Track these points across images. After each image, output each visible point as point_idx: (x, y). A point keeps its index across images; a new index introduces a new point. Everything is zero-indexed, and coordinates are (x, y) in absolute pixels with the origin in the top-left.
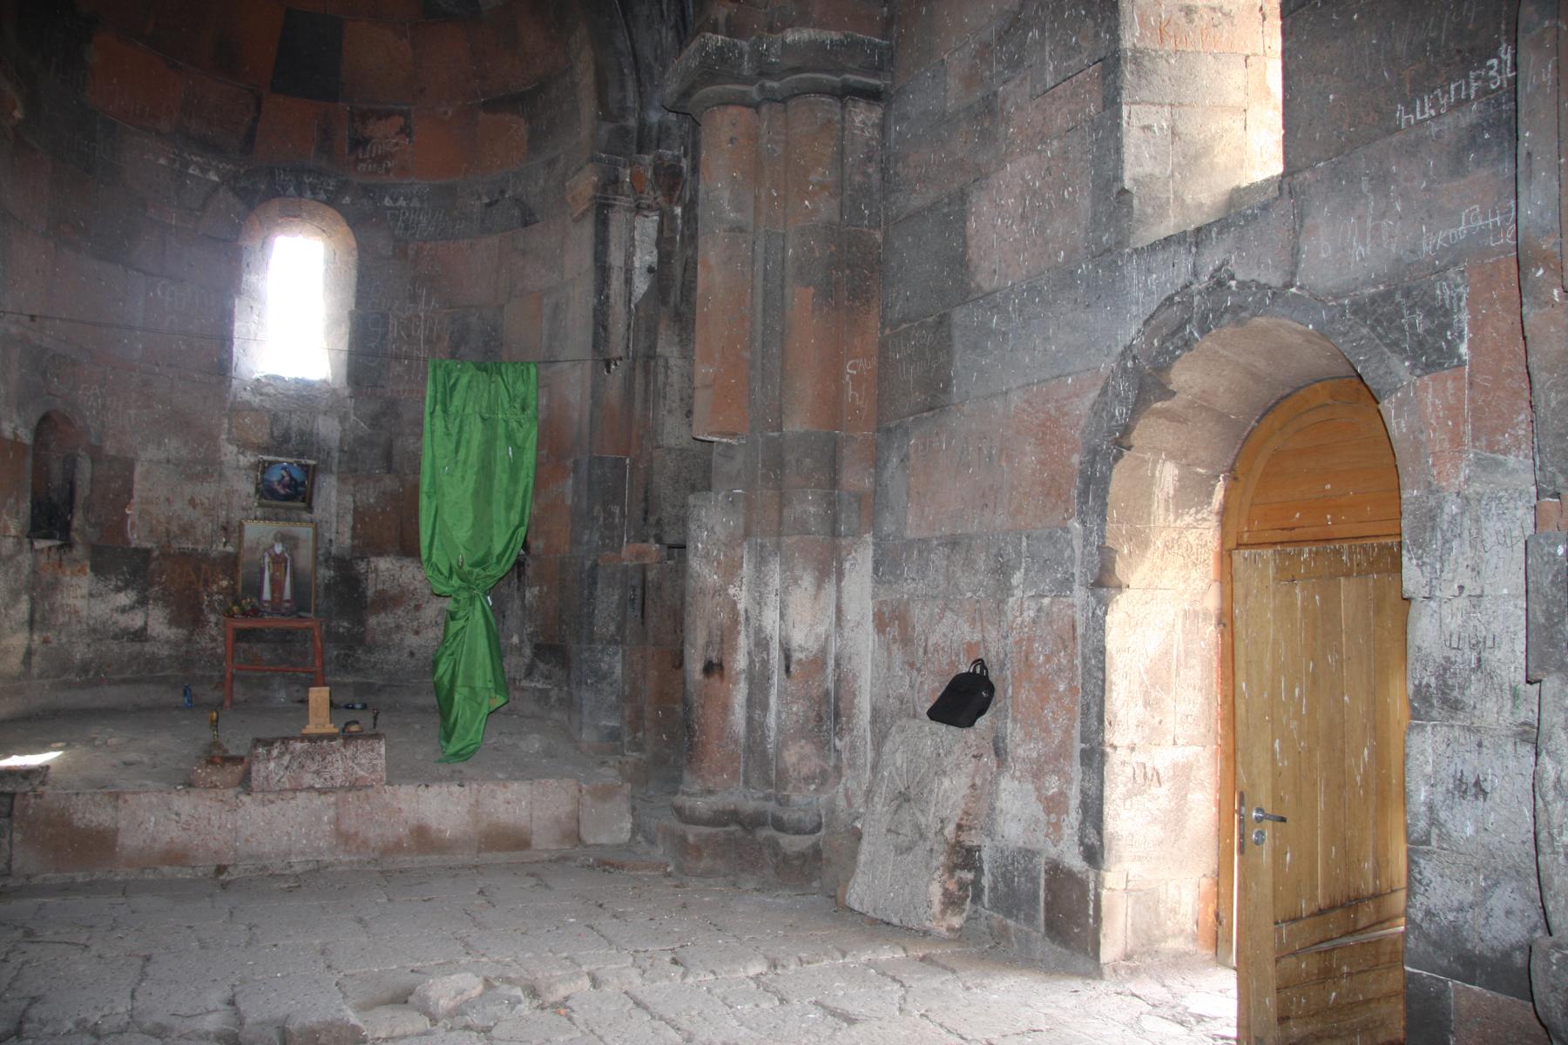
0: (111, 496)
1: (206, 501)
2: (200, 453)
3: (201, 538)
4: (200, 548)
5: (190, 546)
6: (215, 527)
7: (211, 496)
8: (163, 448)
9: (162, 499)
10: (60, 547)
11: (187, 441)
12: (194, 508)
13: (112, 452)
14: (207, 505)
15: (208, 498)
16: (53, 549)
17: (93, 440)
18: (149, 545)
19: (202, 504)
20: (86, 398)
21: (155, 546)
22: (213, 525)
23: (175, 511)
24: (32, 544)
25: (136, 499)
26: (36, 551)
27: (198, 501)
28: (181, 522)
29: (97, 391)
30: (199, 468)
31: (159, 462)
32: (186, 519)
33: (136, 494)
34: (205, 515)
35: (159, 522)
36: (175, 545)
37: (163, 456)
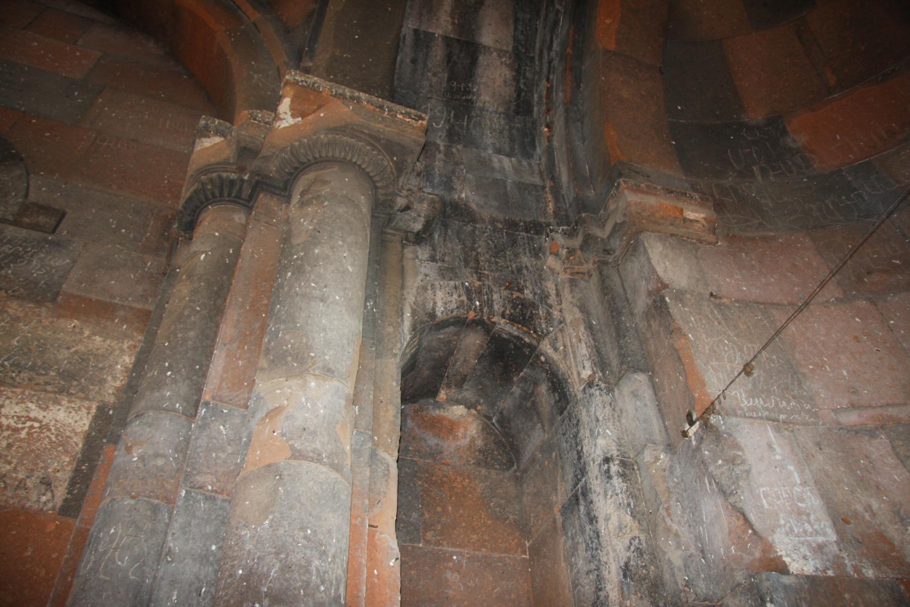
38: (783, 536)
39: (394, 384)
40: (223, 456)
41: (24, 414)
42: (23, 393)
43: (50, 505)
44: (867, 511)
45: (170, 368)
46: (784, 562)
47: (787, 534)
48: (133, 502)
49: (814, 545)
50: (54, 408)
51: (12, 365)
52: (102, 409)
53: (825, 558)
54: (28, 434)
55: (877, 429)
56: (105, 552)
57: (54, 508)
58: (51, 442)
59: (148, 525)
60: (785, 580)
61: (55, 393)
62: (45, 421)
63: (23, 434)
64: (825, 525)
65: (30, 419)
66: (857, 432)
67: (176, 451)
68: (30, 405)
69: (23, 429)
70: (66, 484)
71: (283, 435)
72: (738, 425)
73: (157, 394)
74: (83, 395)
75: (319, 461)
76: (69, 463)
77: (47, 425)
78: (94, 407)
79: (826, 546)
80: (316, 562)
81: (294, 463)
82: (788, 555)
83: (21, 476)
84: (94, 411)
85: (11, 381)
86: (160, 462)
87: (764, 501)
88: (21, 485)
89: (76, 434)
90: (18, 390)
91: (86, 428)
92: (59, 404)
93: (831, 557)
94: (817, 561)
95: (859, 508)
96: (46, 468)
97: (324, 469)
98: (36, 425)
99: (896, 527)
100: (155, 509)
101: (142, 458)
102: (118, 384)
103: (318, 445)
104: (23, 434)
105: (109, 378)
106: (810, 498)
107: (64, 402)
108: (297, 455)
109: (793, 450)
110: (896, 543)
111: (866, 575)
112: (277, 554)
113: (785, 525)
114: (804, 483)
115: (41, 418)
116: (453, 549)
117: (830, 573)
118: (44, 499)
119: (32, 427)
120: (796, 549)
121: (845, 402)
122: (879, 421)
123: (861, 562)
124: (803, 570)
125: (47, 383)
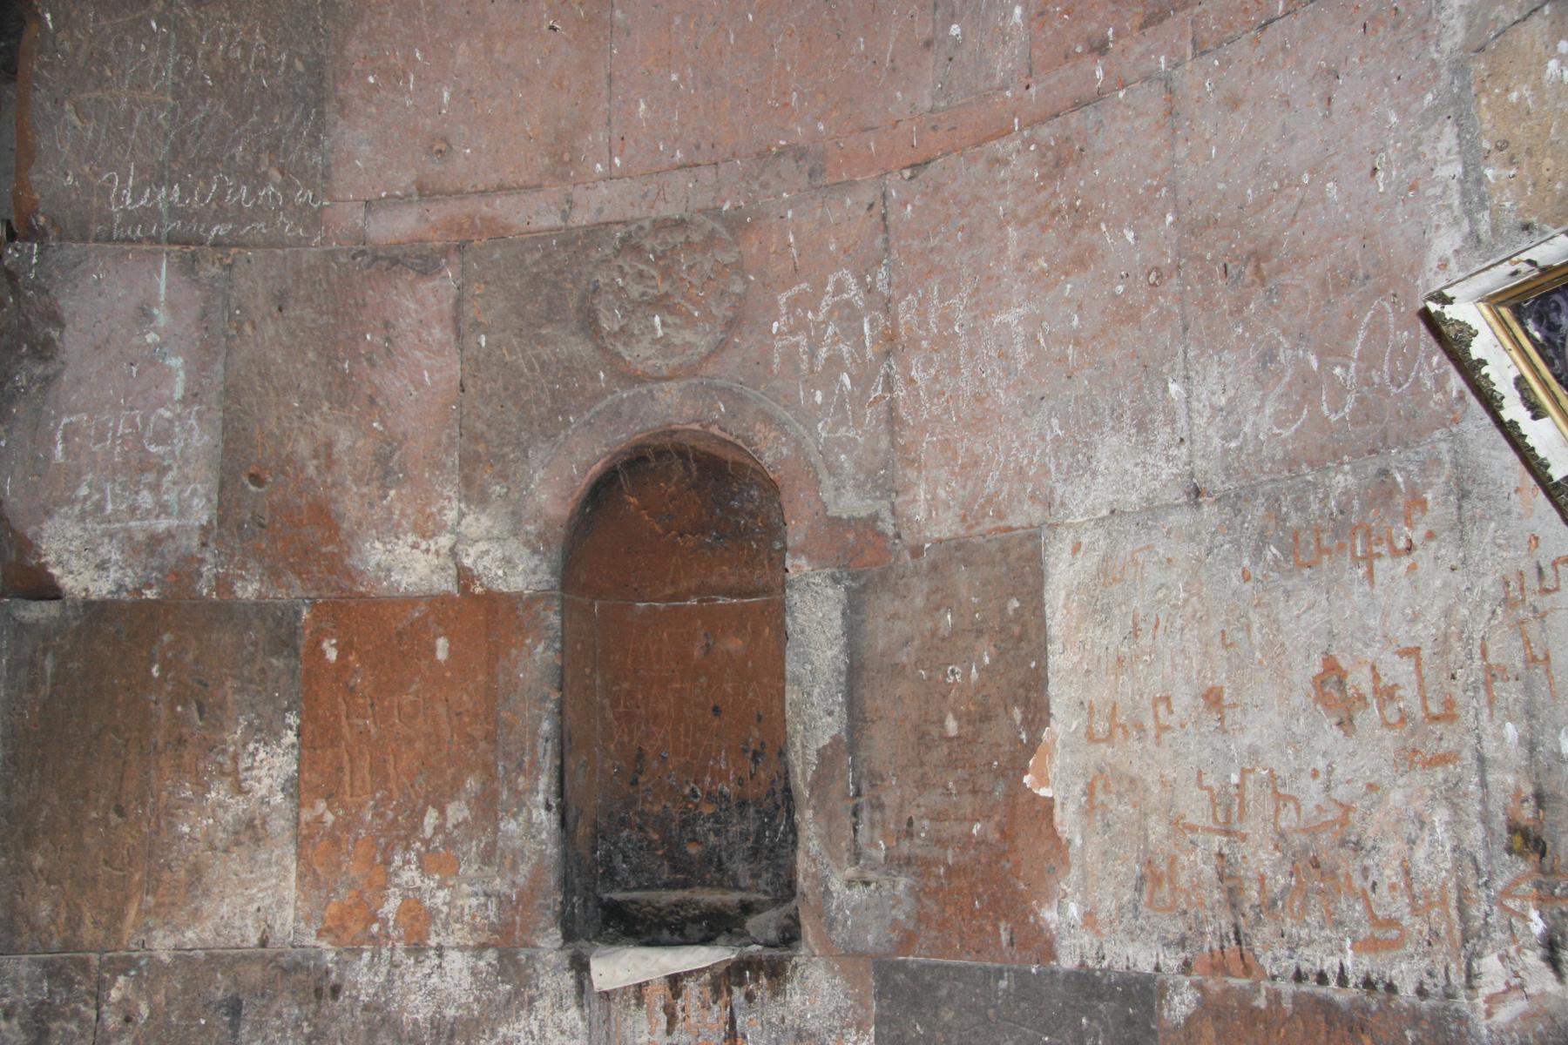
0: (952, 726)
1: (1400, 671)
2: (1339, 392)
3: (1400, 907)
4: (1405, 974)
5: (1355, 963)
6: (1476, 834)
7: (1425, 633)
8: (1163, 436)
9: (1183, 699)
10: (725, 979)
11: (1268, 356)
12: (1346, 724)
13: (946, 526)
14: (1409, 696)
15: (1412, 652)
16: (692, 988)
17: (850, 504)
18: (1142, 958)
19: (1387, 694)
20: (802, 339)
21: (1172, 961)
22: (1456, 822)
23: (1254, 752)
24: (580, 966)
25: (1062, 726)
26: (606, 996)
27: (1360, 680)
28: (1288, 819)
29: (853, 292)
30: (1342, 480)
31: (1152, 511)
32: (1312, 793)
33: (1060, 695)
34: (1409, 758)
35: (1178, 825)
36: (1273, 959)
37: (1167, 471)
38: (68, 523)
44: (316, 457)
46: (51, 576)
47: (82, 518)
49: (140, 537)
53: (155, 562)
55: (445, 252)
60: (36, 612)
64: (194, 493)
66: (395, 261)
72: (76, 265)
79: (173, 537)
82: (59, 563)
87: (60, 447)
93: (171, 560)
94: (129, 572)
95: (303, 447)
99: (365, 490)
106: (191, 429)
109: (204, 315)
110: (345, 525)
111: (239, 594)
113: (86, 498)
114: (192, 397)
117: (150, 594)
120: (90, 546)
121: (405, 180)
122: (459, 232)
123: (244, 566)
124: (86, 590)
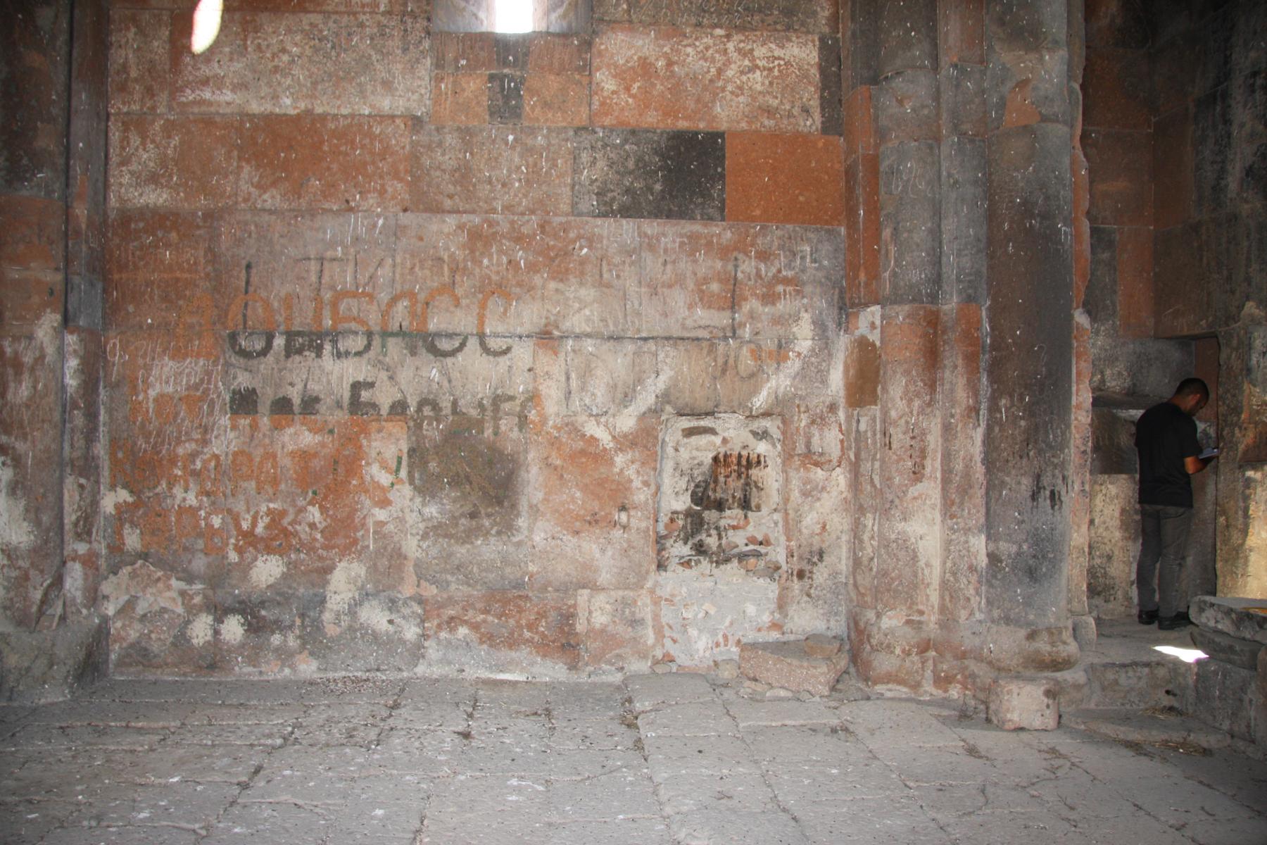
39: (1080, 15)
40: (974, 107)
41: (770, 54)
42: (762, 35)
43: (814, 128)
45: (912, 29)
48: (916, 143)
50: (789, 45)
51: (744, 10)
52: (822, 40)
54: (779, 71)
56: (908, 180)
57: (817, 130)
58: (797, 76)
59: (929, 160)
61: (784, 31)
62: (787, 58)
63: (776, 73)
65: (776, 58)
67: (933, 101)
68: (771, 45)
69: (774, 67)
70: (819, 110)
71: (1033, 103)
73: (909, 54)
74: (805, 30)
75: (1057, 121)
76: (815, 92)
77: (789, 61)
78: (816, 39)
80: (1062, 192)
81: (1043, 125)
83: (788, 107)
84: (817, 43)
85: (748, 26)
86: (926, 112)
88: (790, 115)
89: (812, 66)
90: (758, 33)
91: (817, 60)
92: (791, 41)
96: (801, 98)
97: (1060, 126)
98: (782, 63)
100: (931, 148)
101: (913, 110)
102: (827, 13)
103: (1056, 109)
104: (776, 73)
105: (819, 9)
107: (794, 39)
108: (1044, 119)
112: (1041, 189)
115: (782, 56)
116: (1092, 128)
118: (808, 123)
119: (779, 65)
125: (776, 23)
